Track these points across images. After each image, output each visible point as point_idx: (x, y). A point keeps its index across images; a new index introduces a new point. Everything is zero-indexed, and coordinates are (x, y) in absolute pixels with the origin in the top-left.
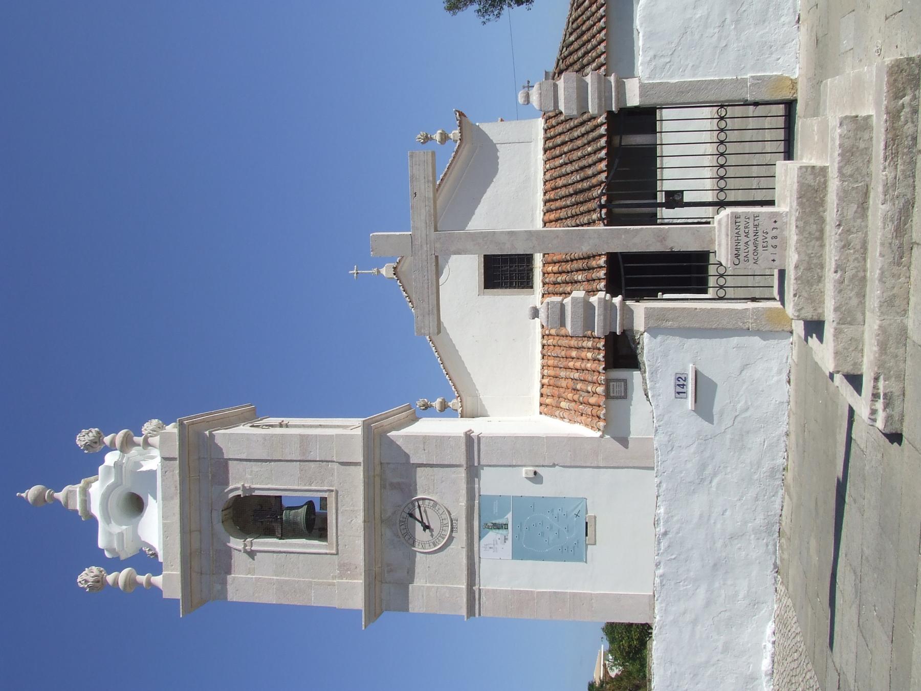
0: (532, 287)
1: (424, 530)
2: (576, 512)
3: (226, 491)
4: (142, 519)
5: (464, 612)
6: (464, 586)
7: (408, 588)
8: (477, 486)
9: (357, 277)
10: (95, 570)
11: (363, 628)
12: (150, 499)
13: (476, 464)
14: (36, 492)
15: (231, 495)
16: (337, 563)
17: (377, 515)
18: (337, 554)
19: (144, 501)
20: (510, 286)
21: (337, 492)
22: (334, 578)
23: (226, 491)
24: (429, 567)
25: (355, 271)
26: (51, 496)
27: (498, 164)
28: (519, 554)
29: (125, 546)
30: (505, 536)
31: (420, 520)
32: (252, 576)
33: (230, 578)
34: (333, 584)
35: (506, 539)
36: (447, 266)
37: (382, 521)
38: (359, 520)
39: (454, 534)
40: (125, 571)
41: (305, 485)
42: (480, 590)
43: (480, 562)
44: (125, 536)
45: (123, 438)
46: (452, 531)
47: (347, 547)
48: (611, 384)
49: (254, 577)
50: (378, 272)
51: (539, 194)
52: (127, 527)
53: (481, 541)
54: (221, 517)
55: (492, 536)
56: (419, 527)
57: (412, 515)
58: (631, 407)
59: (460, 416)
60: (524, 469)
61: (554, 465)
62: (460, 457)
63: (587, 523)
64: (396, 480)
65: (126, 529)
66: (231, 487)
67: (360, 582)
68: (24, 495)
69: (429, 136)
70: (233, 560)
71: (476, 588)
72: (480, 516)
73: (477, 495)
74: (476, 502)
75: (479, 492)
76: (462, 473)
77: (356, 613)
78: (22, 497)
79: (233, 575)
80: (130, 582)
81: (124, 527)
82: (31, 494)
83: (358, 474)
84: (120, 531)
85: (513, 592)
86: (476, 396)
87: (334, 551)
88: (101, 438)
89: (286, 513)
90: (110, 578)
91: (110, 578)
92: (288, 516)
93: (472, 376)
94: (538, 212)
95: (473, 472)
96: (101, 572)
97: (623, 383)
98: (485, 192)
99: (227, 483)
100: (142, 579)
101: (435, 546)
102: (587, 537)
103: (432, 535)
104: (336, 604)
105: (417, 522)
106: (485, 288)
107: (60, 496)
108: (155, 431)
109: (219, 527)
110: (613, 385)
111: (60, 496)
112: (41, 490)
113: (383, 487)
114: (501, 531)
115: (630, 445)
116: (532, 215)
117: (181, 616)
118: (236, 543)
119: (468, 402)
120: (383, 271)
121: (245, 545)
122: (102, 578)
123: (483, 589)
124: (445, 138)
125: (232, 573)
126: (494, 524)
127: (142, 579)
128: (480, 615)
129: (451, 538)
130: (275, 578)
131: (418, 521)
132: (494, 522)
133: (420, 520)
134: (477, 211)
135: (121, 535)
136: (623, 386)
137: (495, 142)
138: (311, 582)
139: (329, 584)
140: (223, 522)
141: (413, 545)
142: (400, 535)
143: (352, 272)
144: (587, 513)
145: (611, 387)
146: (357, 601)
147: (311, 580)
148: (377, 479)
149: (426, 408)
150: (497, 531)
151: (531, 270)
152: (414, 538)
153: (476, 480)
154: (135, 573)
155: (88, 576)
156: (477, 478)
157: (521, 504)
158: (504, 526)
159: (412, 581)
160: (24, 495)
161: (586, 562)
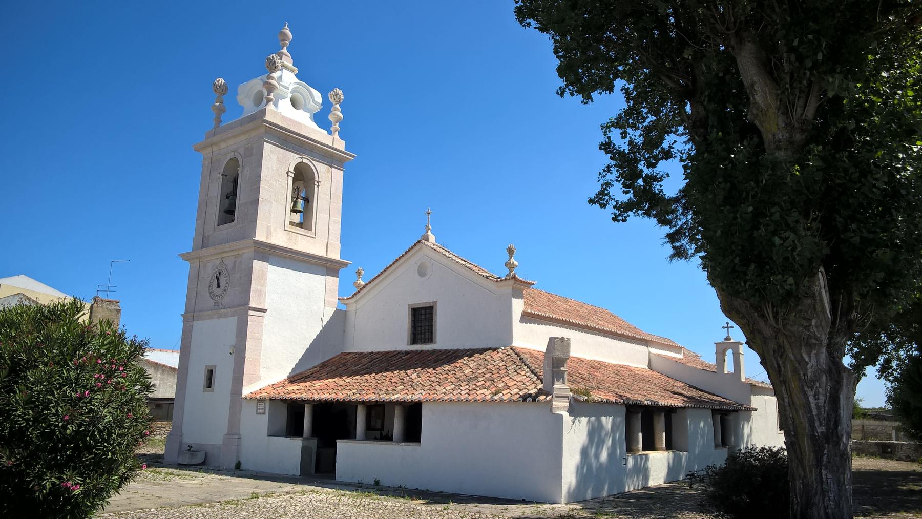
59: (340, 298)
68: (286, 27)
113: (236, 256)
140: (231, 159)
145: (262, 403)
151: (425, 342)
160: (286, 27)
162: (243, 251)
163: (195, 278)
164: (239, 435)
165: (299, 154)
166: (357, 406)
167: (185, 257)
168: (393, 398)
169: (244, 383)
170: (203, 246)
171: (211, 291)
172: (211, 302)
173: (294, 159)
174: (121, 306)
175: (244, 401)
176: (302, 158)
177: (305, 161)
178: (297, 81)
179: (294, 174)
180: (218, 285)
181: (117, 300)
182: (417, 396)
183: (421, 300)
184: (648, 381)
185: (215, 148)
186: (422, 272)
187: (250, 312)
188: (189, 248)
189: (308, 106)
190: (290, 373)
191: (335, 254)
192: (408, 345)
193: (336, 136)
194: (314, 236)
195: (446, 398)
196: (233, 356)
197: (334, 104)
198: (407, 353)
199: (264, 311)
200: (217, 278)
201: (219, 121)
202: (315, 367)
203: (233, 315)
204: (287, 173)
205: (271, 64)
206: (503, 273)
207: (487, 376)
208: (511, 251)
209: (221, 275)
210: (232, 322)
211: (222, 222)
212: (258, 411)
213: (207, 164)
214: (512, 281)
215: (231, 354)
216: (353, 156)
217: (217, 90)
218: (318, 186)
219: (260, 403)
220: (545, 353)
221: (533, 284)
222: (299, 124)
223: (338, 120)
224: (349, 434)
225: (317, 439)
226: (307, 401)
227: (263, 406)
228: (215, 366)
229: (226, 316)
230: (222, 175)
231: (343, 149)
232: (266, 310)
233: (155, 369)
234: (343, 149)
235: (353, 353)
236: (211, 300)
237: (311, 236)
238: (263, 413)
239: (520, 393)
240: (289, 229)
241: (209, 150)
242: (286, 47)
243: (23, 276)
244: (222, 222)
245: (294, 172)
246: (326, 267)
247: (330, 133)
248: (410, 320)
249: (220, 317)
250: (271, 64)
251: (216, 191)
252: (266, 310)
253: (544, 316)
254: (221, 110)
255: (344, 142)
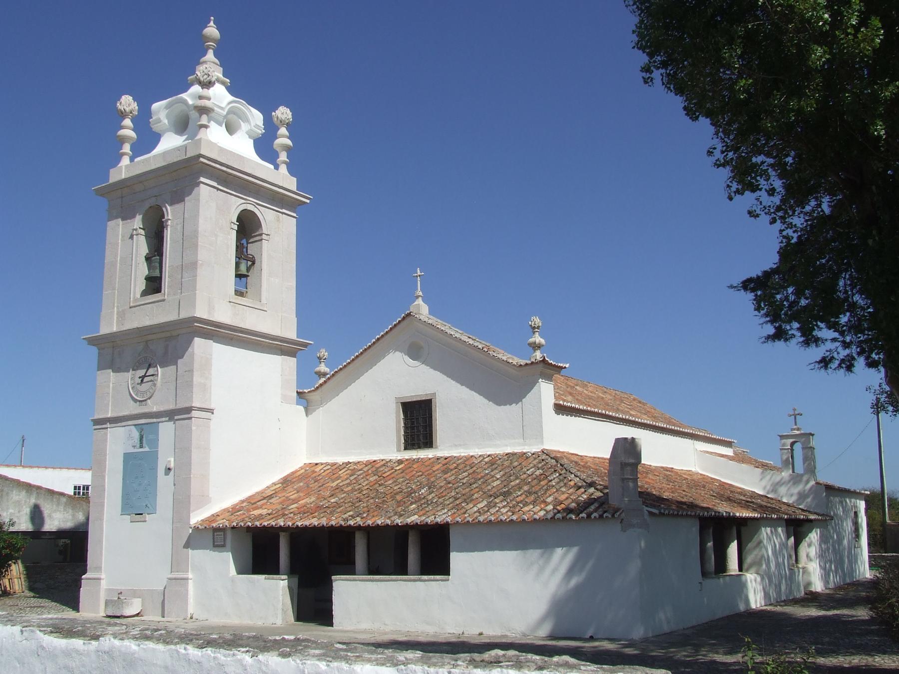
0: (405, 449)
1: (140, 377)
2: (149, 505)
3: (167, 205)
4: (174, 134)
5: (96, 417)
6: (109, 415)
7: (109, 369)
8: (164, 419)
9: (414, 276)
10: (134, 106)
11: (82, 337)
12: (185, 137)
13: (176, 417)
14: (209, 34)
15: (164, 209)
17: (150, 337)
18: (130, 308)
19: (185, 132)
20: (406, 427)
21: (164, 300)
22: (118, 307)
23: (167, 205)
24: (121, 385)
25: (419, 273)
26: (208, 48)
27: (504, 405)
28: (127, 457)
29: (155, 126)
30: (136, 446)
31: (147, 375)
32: (120, 240)
33: (120, 221)
34: (113, 308)
35: (134, 447)
36: (419, 363)
37: (147, 342)
38: (147, 322)
39: (138, 403)
40: (132, 134)
41: (169, 272)
42: (107, 428)
43: (123, 426)
44: (159, 124)
45: (201, 106)
46: (140, 401)
47: (134, 315)
49: (120, 241)
50: (418, 297)
51: (477, 450)
52: (167, 123)
53: (133, 427)
55: (136, 434)
56: (141, 372)
57: (150, 366)
58: (209, 550)
59: (299, 390)
60: (172, 460)
61: (175, 485)
62: (182, 405)
63: (142, 514)
65: (165, 124)
66: (168, 207)
67: (115, 329)
68: (212, 23)
69: (536, 330)
70: (129, 221)
71: (108, 425)
72: (147, 424)
73: (159, 420)
74: (155, 419)
75: (162, 422)
76: (172, 406)
77: (97, 327)
78: (209, 23)
79: (121, 222)
80: (122, 140)
81: (166, 121)
82: (212, 30)
83: (172, 317)
84: (162, 119)
85: (105, 455)
86: (321, 403)
87: (132, 305)
88: (205, 86)
89: (157, 259)
90: (127, 122)
91: (127, 122)
92: (154, 261)
93: (337, 397)
94: (462, 450)
95: (170, 415)
96: (131, 113)
97: (222, 543)
98: (481, 394)
99: (171, 205)
100: (127, 148)
101: (132, 388)
102: (134, 515)
103: (138, 384)
104: (103, 313)
105: (145, 370)
107: (210, 55)
108: (277, 119)
109: (147, 205)
110: (221, 535)
111: (210, 55)
112: (211, 37)
114: (139, 442)
115: (185, 549)
116: (460, 445)
117: (93, 189)
118: (137, 222)
119: (315, 397)
120: (420, 301)
121: (136, 230)
122: (126, 115)
123: (107, 431)
124: (536, 347)
125: (124, 222)
126: (143, 437)
127: (127, 148)
128: (95, 429)
129: (135, 401)
130: (119, 259)
131: (145, 374)
132: (144, 436)
133: (147, 375)
134: (464, 389)
135: (159, 121)
136: (220, 543)
137: (524, 400)
138: (115, 289)
139: (114, 305)
140: (150, 207)
141: (133, 370)
143: (419, 271)
144: (148, 514)
146: (104, 330)
147: (117, 289)
148: (168, 334)
149: (318, 358)
150: (139, 440)
152: (137, 370)
153: (167, 419)
154: (132, 142)
155: (127, 103)
156: (169, 419)
157: (153, 456)
158: (141, 447)
159: (113, 372)
160: (212, 23)
161: (121, 515)
166: (354, 534)
168: (409, 521)
173: (236, 204)
177: (250, 207)
178: (231, 98)
179: (238, 225)
182: (442, 517)
184: (704, 487)
191: (291, 333)
193: (283, 169)
195: (481, 519)
198: (400, 462)
199: (211, 411)
202: (274, 484)
207: (526, 488)
212: (216, 543)
214: (542, 365)
219: (218, 533)
220: (610, 459)
221: (565, 367)
222: (241, 158)
223: (288, 149)
224: (349, 568)
225: (298, 576)
226: (281, 529)
227: (222, 536)
231: (294, 188)
233: (27, 492)
234: (294, 189)
235: (322, 464)
240: (234, 301)
245: (238, 223)
246: (281, 350)
247: (277, 167)
253: (611, 416)
255: (295, 179)
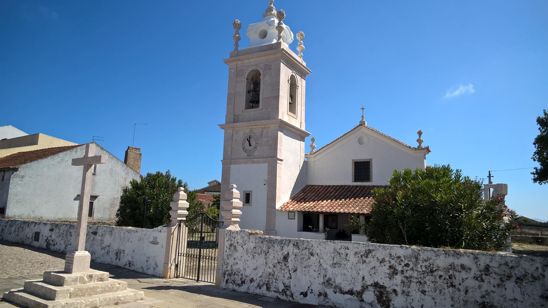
16: (239, 113)
17: (253, 127)
48: (293, 213)
54: (254, 69)
64: (264, 133)
106: (355, 162)
142: (247, 136)
145: (292, 213)
162: (269, 126)
163: (229, 141)
164: (276, 230)
165: (291, 70)
167: (222, 127)
169: (276, 202)
170: (235, 121)
171: (243, 147)
172: (244, 154)
174: (142, 151)
175: (277, 213)
176: (292, 72)
177: (294, 74)
180: (250, 145)
181: (139, 148)
183: (362, 157)
185: (239, 63)
186: (360, 142)
187: (278, 162)
188: (223, 122)
189: (288, 41)
190: (290, 196)
192: (352, 182)
194: (296, 118)
196: (266, 185)
197: (299, 40)
200: (248, 140)
201: (237, 45)
203: (264, 162)
204: (288, 81)
205: (282, 15)
206: (416, 145)
208: (420, 133)
209: (251, 139)
210: (264, 167)
211: (248, 107)
213: (233, 72)
215: (265, 184)
216: (311, 72)
217: (236, 26)
218: (298, 89)
228: (251, 191)
229: (258, 163)
230: (246, 79)
232: (283, 160)
236: (245, 153)
237: (295, 117)
238: (294, 219)
239: (311, 205)
241: (235, 63)
242: (272, 4)
243: (10, 126)
244: (248, 107)
248: (354, 168)
249: (254, 163)
250: (282, 15)
251: (242, 88)
252: (283, 160)
254: (239, 39)
